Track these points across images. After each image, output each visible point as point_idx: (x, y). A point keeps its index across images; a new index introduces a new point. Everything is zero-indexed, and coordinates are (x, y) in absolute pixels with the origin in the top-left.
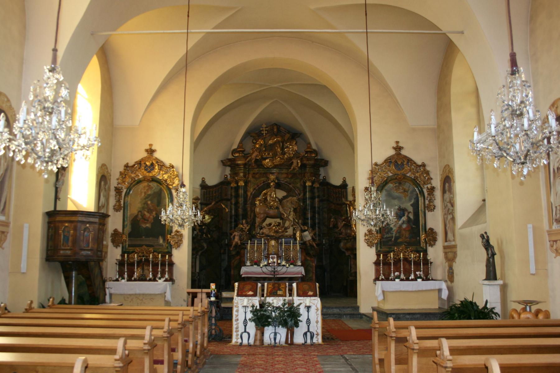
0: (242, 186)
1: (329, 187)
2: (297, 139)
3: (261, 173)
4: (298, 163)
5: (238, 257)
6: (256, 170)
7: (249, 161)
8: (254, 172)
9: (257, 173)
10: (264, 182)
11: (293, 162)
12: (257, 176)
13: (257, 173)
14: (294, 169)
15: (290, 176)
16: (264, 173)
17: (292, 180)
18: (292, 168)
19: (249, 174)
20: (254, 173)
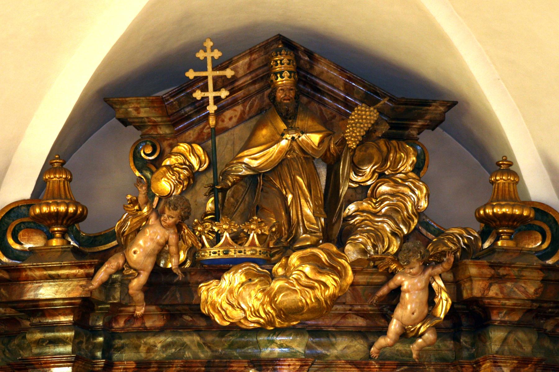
2: (427, 138)
4: (432, 294)
11: (397, 292)
14: (406, 336)
18: (394, 326)
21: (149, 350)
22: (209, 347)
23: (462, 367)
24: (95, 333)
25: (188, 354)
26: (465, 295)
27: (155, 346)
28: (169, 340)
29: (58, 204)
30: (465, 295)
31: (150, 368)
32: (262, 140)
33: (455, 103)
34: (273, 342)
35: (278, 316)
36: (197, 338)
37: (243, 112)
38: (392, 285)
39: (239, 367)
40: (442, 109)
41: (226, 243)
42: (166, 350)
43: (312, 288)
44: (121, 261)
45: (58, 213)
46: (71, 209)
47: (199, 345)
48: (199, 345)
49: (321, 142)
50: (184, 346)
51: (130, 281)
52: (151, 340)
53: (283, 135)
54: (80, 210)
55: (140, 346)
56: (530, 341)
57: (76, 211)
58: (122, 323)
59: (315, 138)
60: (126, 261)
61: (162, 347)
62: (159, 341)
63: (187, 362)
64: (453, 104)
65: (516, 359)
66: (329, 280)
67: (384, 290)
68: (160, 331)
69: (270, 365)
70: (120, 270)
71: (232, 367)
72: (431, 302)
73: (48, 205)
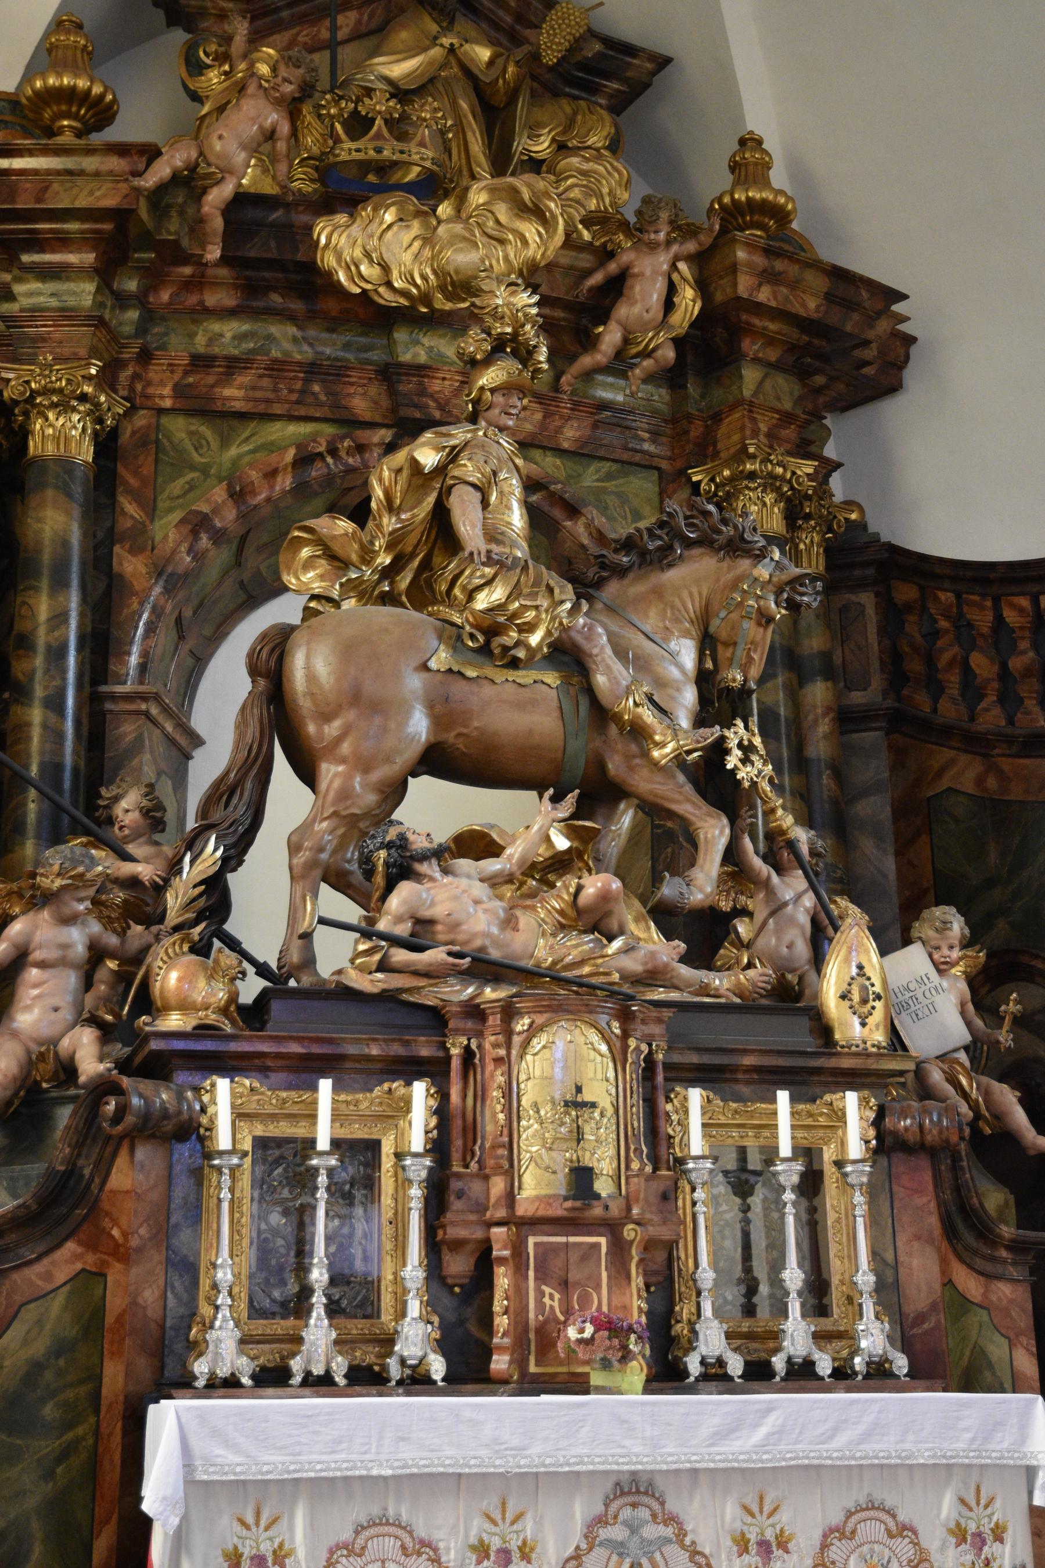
0: (66, 464)
1: (906, 593)
3: (277, 368)
4: (672, 289)
5: (66, 1261)
6: (227, 334)
7: (159, 195)
8: (200, 343)
9: (234, 365)
10: (305, 460)
11: (617, 286)
12: (234, 394)
13: (234, 365)
15: (570, 434)
16: (312, 369)
17: (591, 476)
18: (610, 337)
19: (145, 356)
20: (201, 362)
21: (211, 341)
22: (311, 345)
23: (691, 423)
24: (122, 300)
25: (275, 353)
26: (719, 297)
27: (222, 335)
28: (246, 327)
29: (77, 76)
30: (719, 297)
31: (214, 366)
32: (401, 47)
33: (667, 61)
34: (418, 342)
35: (442, 288)
36: (292, 330)
37: (359, 22)
38: (613, 267)
39: (360, 378)
40: (649, 66)
41: (379, 136)
42: (240, 344)
43: (502, 242)
44: (194, 154)
45: (73, 89)
46: (97, 90)
47: (295, 340)
48: (295, 340)
49: (491, 62)
50: (270, 338)
51: (204, 191)
52: (216, 327)
53: (436, 38)
54: (109, 97)
55: (196, 334)
56: (791, 394)
57: (102, 96)
58: (165, 296)
59: (484, 53)
60: (201, 154)
61: (234, 338)
62: (229, 329)
63: (275, 361)
64: (663, 62)
65: (778, 412)
66: (531, 230)
67: (597, 278)
68: (232, 313)
69: (414, 375)
70: (193, 168)
71: (349, 376)
72: (669, 305)
73: (59, 75)
